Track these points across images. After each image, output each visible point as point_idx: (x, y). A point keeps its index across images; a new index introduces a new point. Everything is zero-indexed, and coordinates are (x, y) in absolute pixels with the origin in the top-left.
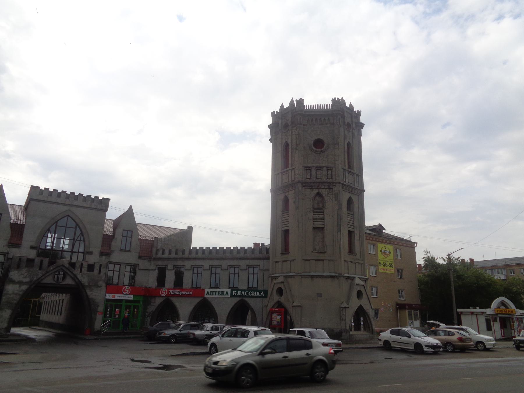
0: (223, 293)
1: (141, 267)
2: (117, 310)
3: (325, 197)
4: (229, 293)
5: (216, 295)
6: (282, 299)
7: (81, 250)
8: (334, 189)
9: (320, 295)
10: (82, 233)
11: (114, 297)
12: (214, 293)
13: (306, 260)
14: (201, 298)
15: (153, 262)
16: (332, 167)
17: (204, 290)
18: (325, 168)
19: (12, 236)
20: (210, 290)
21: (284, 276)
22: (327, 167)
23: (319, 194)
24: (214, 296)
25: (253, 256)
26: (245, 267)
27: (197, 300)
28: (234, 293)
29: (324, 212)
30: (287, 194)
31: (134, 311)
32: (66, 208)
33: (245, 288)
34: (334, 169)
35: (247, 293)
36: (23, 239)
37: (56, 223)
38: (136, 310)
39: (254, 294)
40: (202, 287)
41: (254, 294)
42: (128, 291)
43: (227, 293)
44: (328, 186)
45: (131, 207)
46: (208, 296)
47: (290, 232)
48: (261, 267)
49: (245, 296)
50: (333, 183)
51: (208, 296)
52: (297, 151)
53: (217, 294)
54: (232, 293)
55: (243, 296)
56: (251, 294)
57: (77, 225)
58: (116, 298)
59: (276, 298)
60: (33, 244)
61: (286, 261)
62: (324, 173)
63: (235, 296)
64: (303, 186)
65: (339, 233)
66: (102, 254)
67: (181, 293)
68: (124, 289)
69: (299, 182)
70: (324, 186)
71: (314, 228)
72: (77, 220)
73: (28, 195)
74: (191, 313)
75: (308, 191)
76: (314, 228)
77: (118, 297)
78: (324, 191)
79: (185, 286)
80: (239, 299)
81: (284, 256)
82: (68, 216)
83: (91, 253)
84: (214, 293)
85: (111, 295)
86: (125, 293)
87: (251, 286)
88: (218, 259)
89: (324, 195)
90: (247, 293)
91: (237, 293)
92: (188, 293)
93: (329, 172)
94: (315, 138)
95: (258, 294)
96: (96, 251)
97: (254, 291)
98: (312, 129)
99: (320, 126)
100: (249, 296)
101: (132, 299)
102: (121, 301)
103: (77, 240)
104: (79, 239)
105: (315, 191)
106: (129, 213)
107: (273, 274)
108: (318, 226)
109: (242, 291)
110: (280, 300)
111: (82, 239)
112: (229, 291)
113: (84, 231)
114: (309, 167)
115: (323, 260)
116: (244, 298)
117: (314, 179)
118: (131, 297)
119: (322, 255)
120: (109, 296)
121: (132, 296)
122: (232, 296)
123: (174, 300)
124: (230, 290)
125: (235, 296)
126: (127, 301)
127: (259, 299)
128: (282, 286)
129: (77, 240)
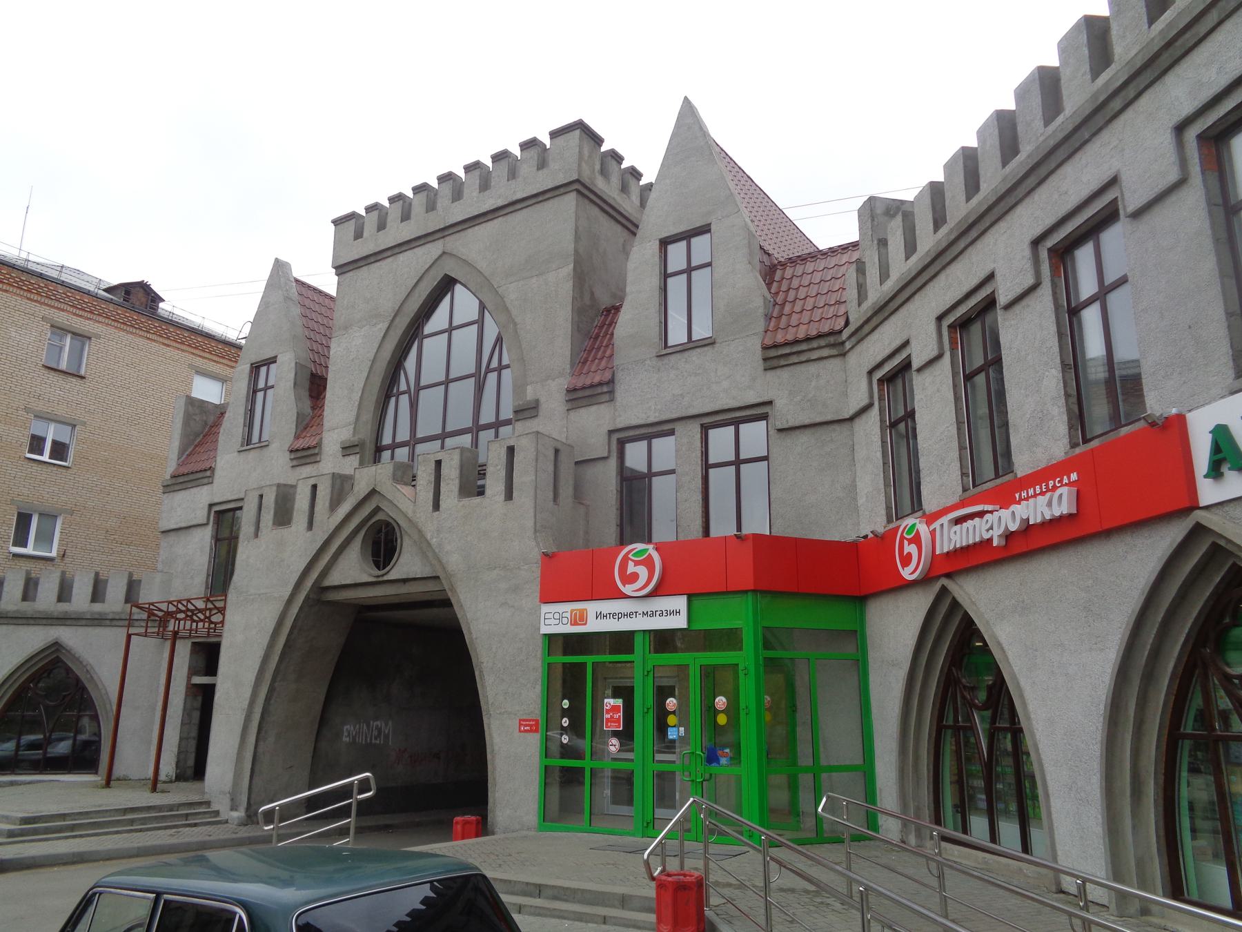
1: (787, 411)
11: (580, 618)
17: (1176, 427)
31: (710, 711)
38: (721, 701)
42: (643, 571)
58: (594, 626)
66: (579, 396)
68: (626, 560)
77: (599, 617)
79: (1024, 462)
85: (566, 608)
86: (628, 589)
96: (552, 395)
101: (679, 622)
102: (622, 641)
103: (488, 370)
104: (494, 364)
118: (672, 613)
120: (557, 619)
121: (680, 603)
126: (663, 640)
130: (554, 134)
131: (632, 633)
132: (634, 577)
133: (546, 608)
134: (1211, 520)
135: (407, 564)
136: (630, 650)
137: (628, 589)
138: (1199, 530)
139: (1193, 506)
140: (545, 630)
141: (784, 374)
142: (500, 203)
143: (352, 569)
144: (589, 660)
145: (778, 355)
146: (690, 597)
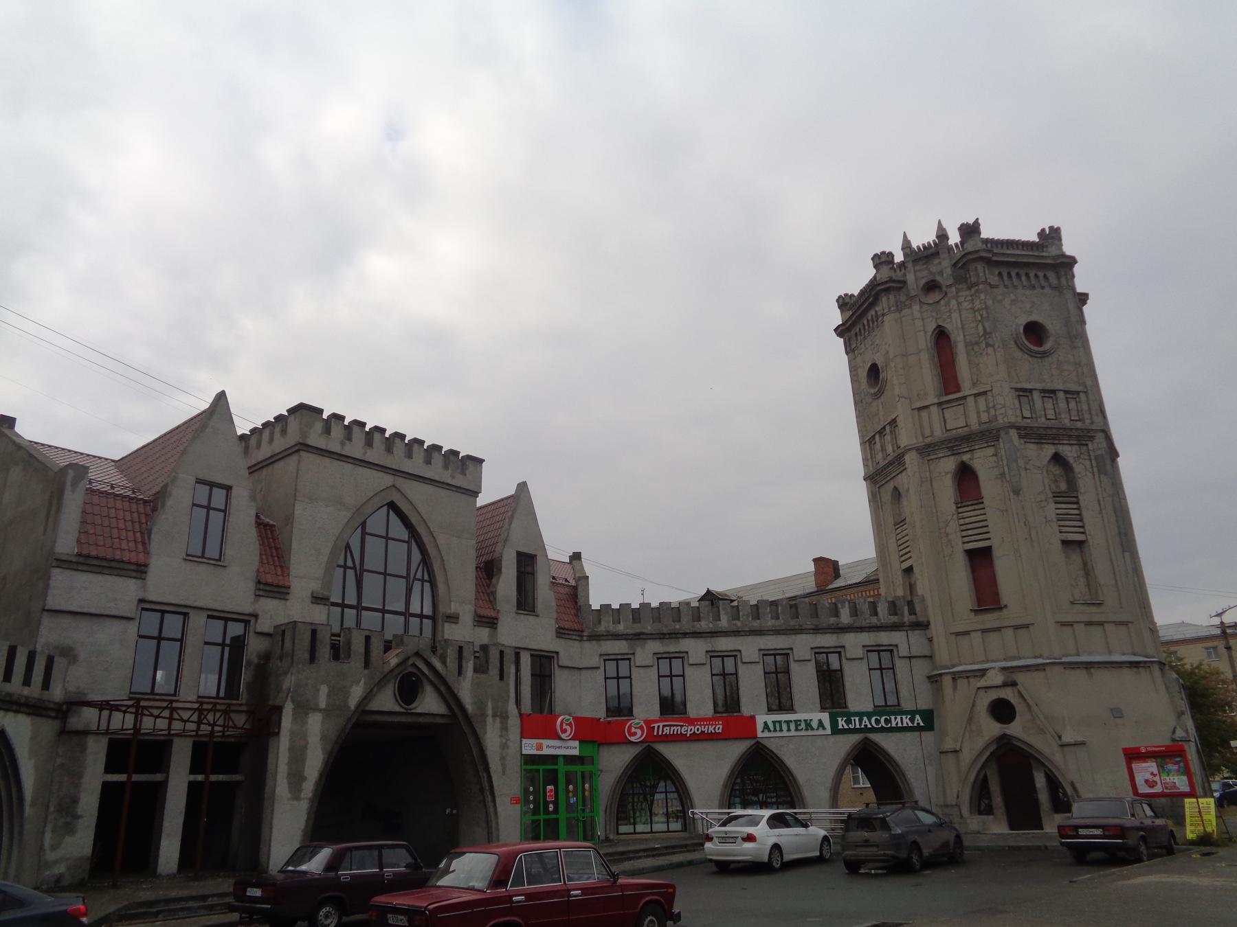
0: (808, 725)
1: (564, 660)
2: (549, 787)
3: (1074, 465)
4: (827, 723)
5: (789, 730)
6: (1015, 729)
7: (427, 610)
8: (1090, 446)
9: (1117, 713)
10: (426, 561)
11: (540, 747)
12: (784, 727)
13: (1063, 624)
15: (587, 645)
16: (1078, 393)
17: (753, 718)
18: (1061, 395)
19: (261, 562)
20: (770, 718)
21: (1004, 669)
22: (1066, 392)
23: (1057, 458)
24: (785, 733)
25: (874, 620)
26: (859, 653)
27: (737, 749)
28: (841, 723)
29: (1077, 503)
30: (965, 458)
32: (388, 480)
33: (869, 707)
34: (1082, 395)
35: (878, 721)
36: (293, 572)
37: (363, 524)
38: (587, 786)
39: (895, 721)
40: (746, 710)
41: (895, 721)
42: (568, 728)
43: (821, 724)
44: (1079, 438)
45: (522, 487)
46: (766, 734)
47: (996, 553)
48: (903, 651)
49: (873, 730)
50: (1089, 430)
51: (766, 734)
52: (990, 350)
54: (834, 723)
55: (866, 730)
56: (887, 721)
57: (414, 534)
58: (546, 751)
59: (992, 729)
60: (316, 586)
61: (998, 629)
62: (1063, 405)
63: (844, 731)
64: (1020, 437)
65: (1127, 554)
67: (688, 730)
69: (1012, 426)
70: (1070, 437)
71: (1065, 543)
72: (414, 519)
73: (306, 432)
74: (725, 786)
75: (1031, 450)
76: (1065, 543)
77: (549, 747)
78: (1069, 452)
79: (692, 712)
80: (856, 738)
81: (980, 618)
82: (392, 506)
83: (453, 618)
84: (784, 727)
87: (881, 702)
88: (777, 632)
89: (1071, 460)
90: (878, 721)
91: (848, 722)
92: (711, 729)
93: (1072, 404)
94: (1023, 320)
95: (906, 721)
96: (467, 616)
97: (896, 714)
98: (1012, 296)
99: (1028, 292)
100: (883, 730)
101: (576, 752)
102: (554, 759)
103: (415, 579)
104: (419, 575)
105: (1049, 450)
106: (519, 502)
107: (954, 666)
108: (1071, 537)
109: (861, 715)
110: (1008, 732)
111: (426, 577)
112: (825, 717)
113: (432, 551)
114: (1025, 390)
115: (1101, 624)
117: (1043, 419)
118: (573, 748)
119: (1093, 609)
120: (530, 747)
121: (576, 743)
122: (836, 731)
123: (667, 750)
124: (827, 715)
125: (844, 731)
126: (569, 759)
127: (908, 734)
128: (1008, 694)
129: (415, 579)
130: (469, 457)
131: (556, 757)
132: (564, 731)
133: (524, 741)
135: (430, 703)
136: (556, 764)
137: (563, 736)
139: (756, 737)
140: (524, 752)
141: (563, 641)
142: (437, 478)
143: (386, 701)
144: (541, 768)
145: (561, 633)
146: (581, 742)
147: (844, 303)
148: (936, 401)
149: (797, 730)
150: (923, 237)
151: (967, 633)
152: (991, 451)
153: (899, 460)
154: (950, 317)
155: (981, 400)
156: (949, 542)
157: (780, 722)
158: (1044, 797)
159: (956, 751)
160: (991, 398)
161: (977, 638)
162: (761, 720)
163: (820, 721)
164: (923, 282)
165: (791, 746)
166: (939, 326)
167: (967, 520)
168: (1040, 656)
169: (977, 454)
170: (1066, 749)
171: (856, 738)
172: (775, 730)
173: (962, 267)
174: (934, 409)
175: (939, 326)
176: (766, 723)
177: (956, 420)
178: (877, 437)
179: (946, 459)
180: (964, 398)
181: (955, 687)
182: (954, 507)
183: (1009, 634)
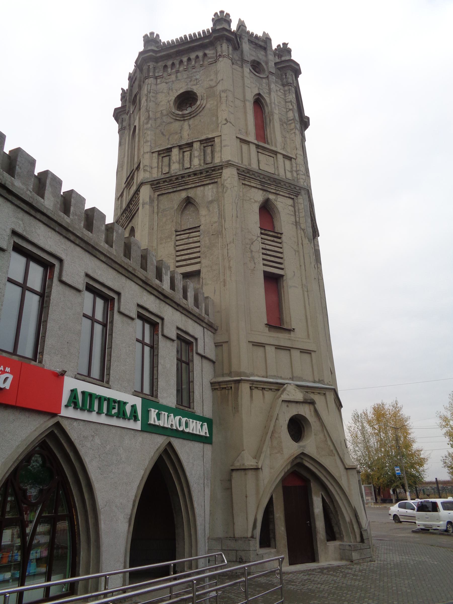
14: (53, 421)
21: (298, 386)
30: (272, 197)
40: (51, 362)
53: (128, 409)
54: (146, 413)
107: (252, 375)
116: (177, 443)
134: (65, 424)
138: (58, 425)
139: (54, 415)
147: (151, 40)
148: (256, 142)
149: (109, 415)
150: (255, 28)
151: (262, 345)
152: (290, 202)
153: (211, 174)
154: (270, 93)
155: (287, 162)
156: (253, 258)
157: (91, 395)
158: (320, 524)
159: (257, 469)
160: (294, 165)
161: (270, 350)
162: (70, 384)
163: (133, 407)
164: (253, 58)
165: (97, 441)
166: (259, 94)
167: (268, 247)
168: (319, 382)
169: (280, 199)
170: (348, 471)
171: (159, 441)
172: (82, 409)
173: (279, 69)
174: (253, 147)
175: (259, 94)
176: (73, 392)
177: (267, 165)
178: (175, 151)
179: (256, 190)
180: (276, 153)
181: (251, 396)
182: (259, 231)
183: (296, 354)
